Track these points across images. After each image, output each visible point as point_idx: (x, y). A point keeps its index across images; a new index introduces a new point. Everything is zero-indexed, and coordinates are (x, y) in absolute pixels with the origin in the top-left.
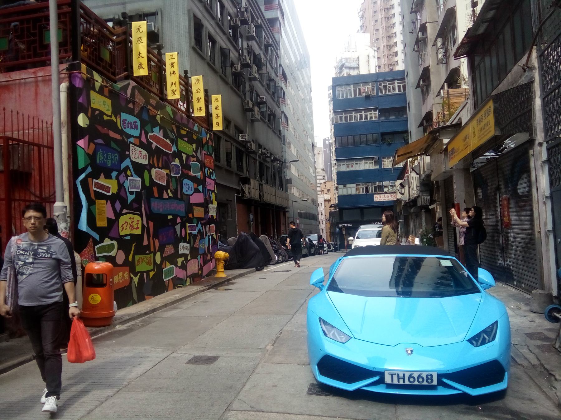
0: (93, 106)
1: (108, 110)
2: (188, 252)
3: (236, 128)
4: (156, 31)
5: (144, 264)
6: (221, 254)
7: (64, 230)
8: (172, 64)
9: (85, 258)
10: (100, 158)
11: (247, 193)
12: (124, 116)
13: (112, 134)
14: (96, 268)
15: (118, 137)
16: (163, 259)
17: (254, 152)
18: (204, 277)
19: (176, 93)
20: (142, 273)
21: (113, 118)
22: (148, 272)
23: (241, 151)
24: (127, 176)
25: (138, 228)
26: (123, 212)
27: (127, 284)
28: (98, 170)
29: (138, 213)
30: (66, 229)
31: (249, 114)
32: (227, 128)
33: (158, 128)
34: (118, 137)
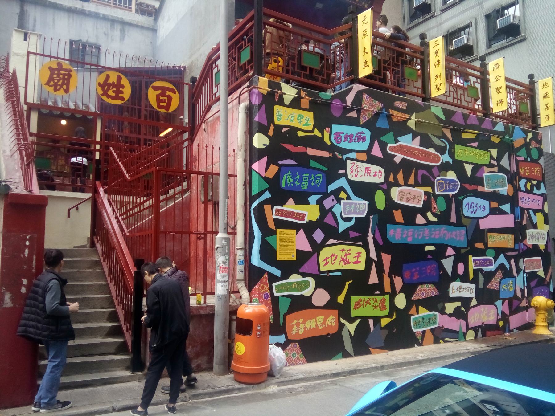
0: (277, 122)
1: (306, 124)
2: (473, 295)
4: (516, 22)
5: (367, 307)
6: (540, 300)
7: (222, 264)
8: (437, 53)
9: (255, 297)
10: (287, 180)
12: (336, 128)
13: (311, 152)
14: (247, 311)
15: (325, 154)
16: (410, 303)
18: (510, 331)
19: (441, 87)
20: (364, 320)
21: (317, 133)
22: (377, 320)
24: (339, 200)
25: (357, 262)
26: (328, 243)
27: (334, 331)
28: (279, 196)
29: (361, 243)
30: (224, 263)
33: (410, 135)
34: (325, 154)
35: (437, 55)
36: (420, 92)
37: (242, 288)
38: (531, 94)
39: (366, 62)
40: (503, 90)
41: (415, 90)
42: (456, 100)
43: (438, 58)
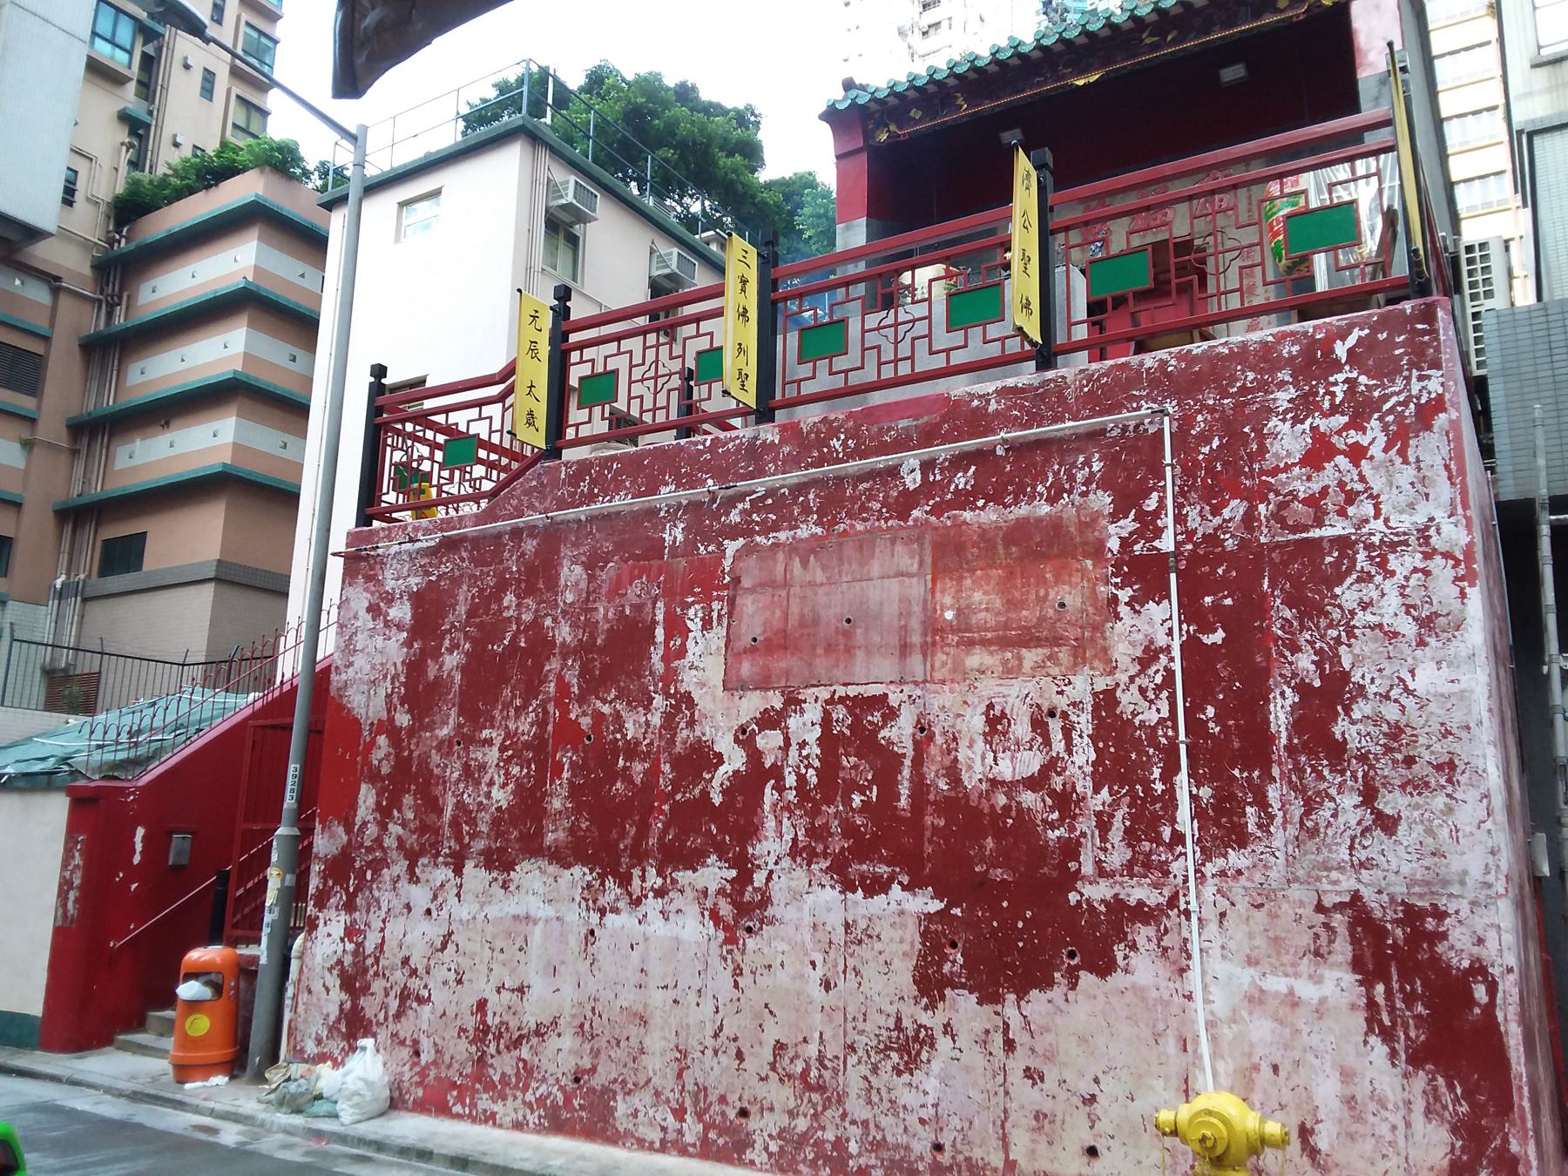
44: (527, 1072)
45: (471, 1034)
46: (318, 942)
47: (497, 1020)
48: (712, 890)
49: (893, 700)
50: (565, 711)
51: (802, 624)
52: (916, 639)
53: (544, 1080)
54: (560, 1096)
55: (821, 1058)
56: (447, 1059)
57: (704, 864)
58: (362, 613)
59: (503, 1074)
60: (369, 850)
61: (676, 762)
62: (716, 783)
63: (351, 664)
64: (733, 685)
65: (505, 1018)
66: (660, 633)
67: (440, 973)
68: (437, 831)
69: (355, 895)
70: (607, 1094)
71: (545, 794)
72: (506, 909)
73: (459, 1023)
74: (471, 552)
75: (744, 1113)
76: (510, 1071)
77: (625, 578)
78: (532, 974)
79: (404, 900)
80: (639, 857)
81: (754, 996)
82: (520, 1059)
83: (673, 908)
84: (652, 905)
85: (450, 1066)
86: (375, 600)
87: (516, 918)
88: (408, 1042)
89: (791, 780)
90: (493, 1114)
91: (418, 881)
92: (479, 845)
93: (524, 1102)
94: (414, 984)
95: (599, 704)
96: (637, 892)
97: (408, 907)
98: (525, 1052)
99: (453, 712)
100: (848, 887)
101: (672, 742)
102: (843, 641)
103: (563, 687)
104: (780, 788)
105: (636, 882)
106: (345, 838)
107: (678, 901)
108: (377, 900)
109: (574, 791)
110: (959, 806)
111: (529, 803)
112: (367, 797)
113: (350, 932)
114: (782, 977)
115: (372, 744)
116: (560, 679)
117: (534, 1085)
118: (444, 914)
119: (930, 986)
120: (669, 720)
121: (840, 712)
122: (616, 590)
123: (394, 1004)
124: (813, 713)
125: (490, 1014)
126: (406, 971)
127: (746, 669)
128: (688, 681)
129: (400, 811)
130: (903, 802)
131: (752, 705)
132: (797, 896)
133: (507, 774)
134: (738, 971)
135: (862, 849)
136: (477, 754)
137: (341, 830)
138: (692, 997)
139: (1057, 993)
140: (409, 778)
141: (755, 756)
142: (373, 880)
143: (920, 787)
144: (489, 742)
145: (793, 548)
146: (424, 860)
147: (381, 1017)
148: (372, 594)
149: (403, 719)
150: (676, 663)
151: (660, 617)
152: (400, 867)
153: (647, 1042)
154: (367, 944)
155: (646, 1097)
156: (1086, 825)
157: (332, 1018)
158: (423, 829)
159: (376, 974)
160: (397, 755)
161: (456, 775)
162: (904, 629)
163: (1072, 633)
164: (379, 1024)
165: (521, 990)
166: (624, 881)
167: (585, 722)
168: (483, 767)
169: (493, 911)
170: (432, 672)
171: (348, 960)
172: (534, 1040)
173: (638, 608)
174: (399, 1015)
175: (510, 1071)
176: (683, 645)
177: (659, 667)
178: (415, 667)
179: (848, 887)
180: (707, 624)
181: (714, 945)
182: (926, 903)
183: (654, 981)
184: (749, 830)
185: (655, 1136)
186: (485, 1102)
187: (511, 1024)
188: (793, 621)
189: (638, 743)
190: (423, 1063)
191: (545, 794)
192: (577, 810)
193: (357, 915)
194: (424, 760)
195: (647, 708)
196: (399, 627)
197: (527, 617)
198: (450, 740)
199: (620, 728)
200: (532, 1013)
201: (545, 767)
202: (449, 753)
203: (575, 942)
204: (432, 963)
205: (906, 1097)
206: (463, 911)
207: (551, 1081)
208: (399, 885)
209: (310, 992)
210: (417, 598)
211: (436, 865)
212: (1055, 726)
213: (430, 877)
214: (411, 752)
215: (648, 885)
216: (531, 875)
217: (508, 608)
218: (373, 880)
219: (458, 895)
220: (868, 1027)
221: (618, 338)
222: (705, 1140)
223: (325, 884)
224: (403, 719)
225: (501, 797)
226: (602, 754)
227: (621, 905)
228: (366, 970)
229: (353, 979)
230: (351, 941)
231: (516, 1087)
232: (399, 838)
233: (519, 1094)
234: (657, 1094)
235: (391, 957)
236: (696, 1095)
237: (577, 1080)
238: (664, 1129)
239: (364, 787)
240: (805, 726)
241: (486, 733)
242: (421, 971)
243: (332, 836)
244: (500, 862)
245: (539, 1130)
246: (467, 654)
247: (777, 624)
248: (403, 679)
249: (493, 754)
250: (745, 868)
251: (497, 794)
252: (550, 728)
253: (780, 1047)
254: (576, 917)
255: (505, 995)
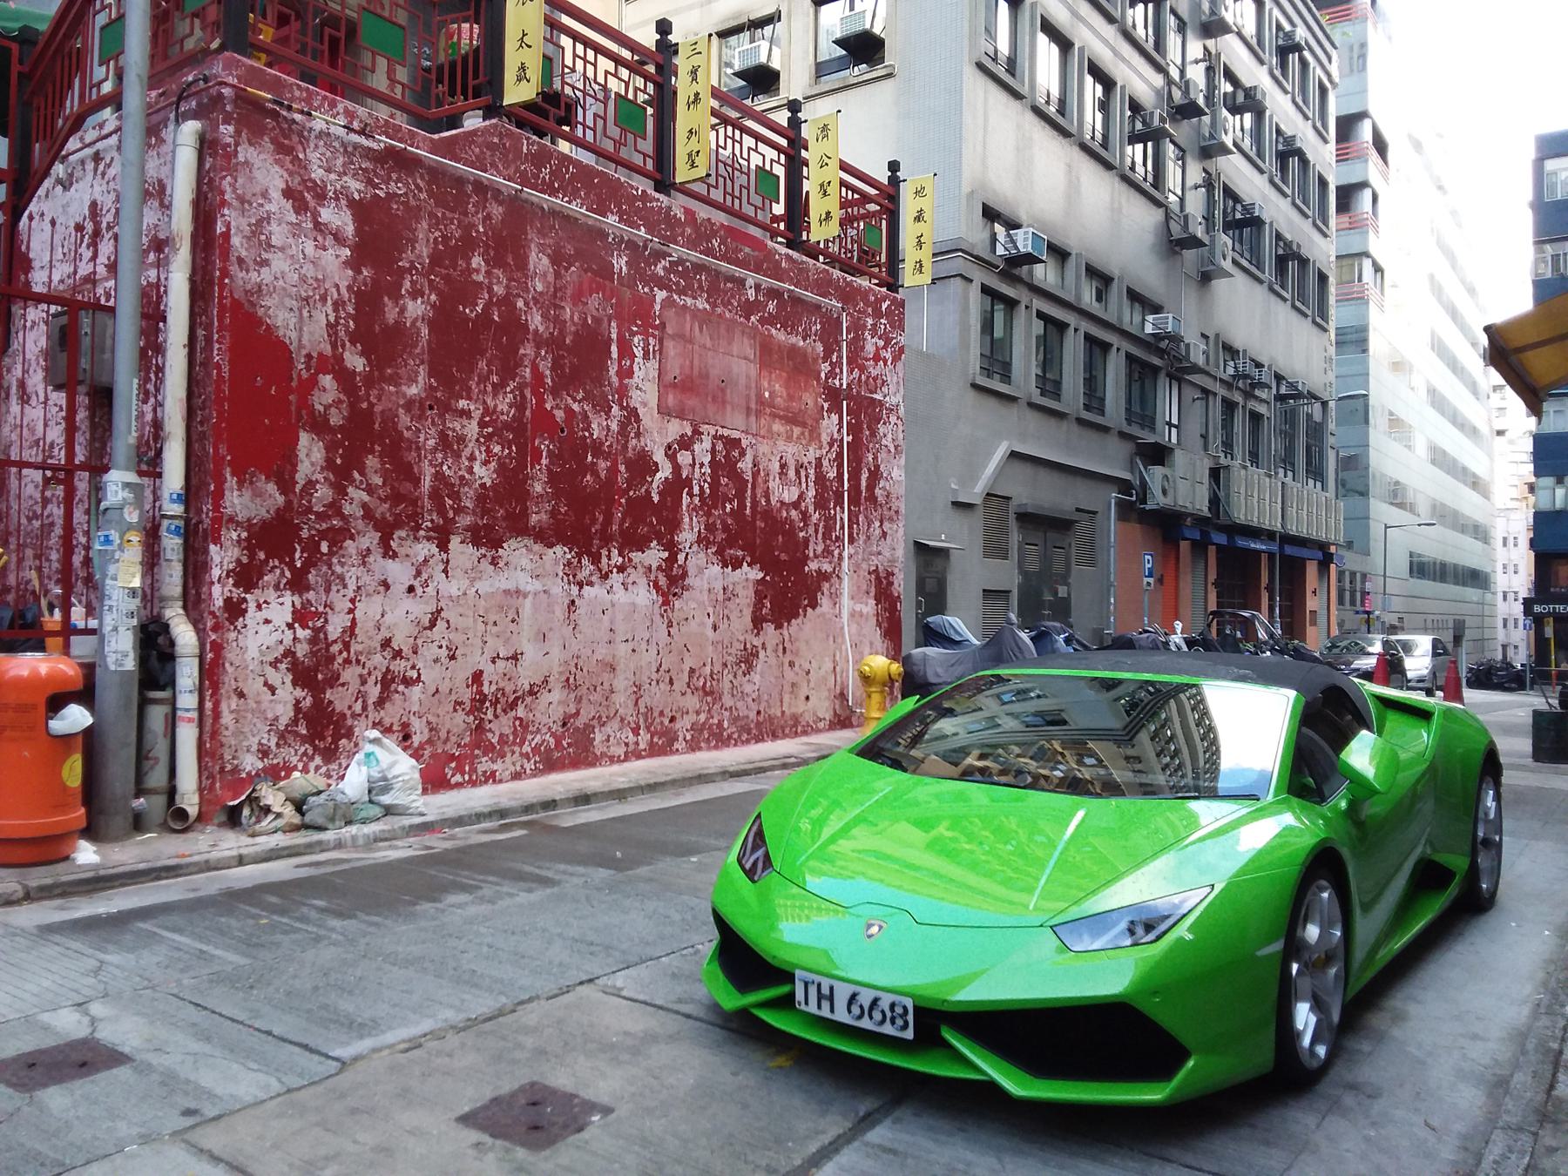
3: (1134, 296)
4: (877, 30)
11: (1158, 492)
17: (1196, 369)
23: (1145, 365)
31: (1189, 255)
32: (1099, 299)
35: (695, 79)
36: (650, 165)
37: (176, 620)
38: (890, 206)
39: (523, 68)
40: (834, 189)
41: (638, 160)
42: (729, 198)
43: (695, 88)
44: (524, 726)
45: (468, 706)
46: (250, 632)
47: (494, 688)
48: (654, 567)
49: (744, 443)
50: (541, 402)
51: (701, 376)
52: (753, 406)
53: (538, 730)
54: (552, 740)
55: (712, 673)
56: (443, 735)
57: (649, 548)
58: (276, 194)
59: (501, 735)
60: (321, 517)
61: (629, 464)
62: (655, 485)
63: (265, 263)
64: (664, 411)
65: (501, 685)
66: (614, 348)
67: (429, 652)
68: (414, 502)
69: (305, 569)
70: (588, 728)
71: (527, 477)
72: (497, 584)
73: (453, 697)
74: (429, 183)
75: (672, 719)
76: (507, 731)
77: (586, 286)
78: (525, 641)
79: (379, 577)
80: (606, 540)
81: (679, 640)
82: (516, 718)
83: (630, 580)
84: (616, 578)
85: (447, 739)
86: (295, 183)
87: (507, 592)
88: (395, 728)
89: (696, 490)
90: (493, 773)
91: (395, 556)
92: (465, 520)
93: (521, 754)
94: (399, 666)
95: (570, 401)
96: (605, 569)
97: (386, 585)
98: (521, 711)
99: (422, 371)
100: (725, 565)
101: (625, 447)
102: (719, 398)
103: (538, 376)
104: (691, 495)
105: (604, 560)
106: (281, 500)
107: (634, 575)
108: (342, 578)
109: (553, 479)
110: (768, 514)
111: (512, 483)
112: (310, 454)
113: (301, 616)
114: (693, 624)
115: (312, 383)
116: (535, 368)
117: (530, 737)
118: (430, 590)
119: (758, 622)
120: (623, 426)
121: (720, 447)
122: (578, 298)
123: (374, 692)
124: (707, 444)
125: (486, 684)
126: (388, 654)
127: (671, 400)
128: (636, 399)
129: (362, 474)
130: (748, 511)
131: (676, 428)
132: (701, 571)
133: (488, 451)
134: (670, 625)
135: (730, 542)
136: (455, 425)
137: (271, 488)
138: (644, 646)
139: (799, 620)
140: (359, 437)
141: (677, 468)
142: (331, 553)
143: (755, 503)
144: (466, 414)
145: (695, 313)
146: (403, 533)
147: (358, 708)
148: (291, 174)
149: (356, 361)
150: (626, 381)
151: (614, 336)
152: (370, 539)
153: (615, 683)
154: (330, 628)
155: (615, 724)
156: (811, 530)
157: (284, 721)
158: (396, 498)
159: (347, 661)
160: (352, 406)
161: (431, 442)
162: (748, 396)
163: (809, 422)
164: (355, 716)
165: (515, 658)
166: (596, 560)
167: (559, 415)
168: (461, 439)
169: (484, 586)
170: (391, 314)
171: (302, 650)
172: (529, 699)
173: (597, 320)
174: (380, 703)
175: (507, 731)
176: (631, 366)
177: (615, 379)
178: (367, 302)
179: (725, 565)
180: (646, 356)
181: (657, 606)
182: (755, 574)
183: (620, 637)
184: (675, 525)
185: (620, 751)
186: (484, 765)
187: (507, 690)
188: (696, 372)
189: (602, 444)
190: (416, 744)
191: (527, 477)
192: (556, 495)
193: (311, 595)
194: (390, 419)
195: (608, 417)
196: (338, 238)
197: (499, 290)
198: (421, 402)
199: (588, 428)
200: (526, 676)
201: (528, 454)
202: (421, 417)
203: (560, 612)
204: (419, 642)
205: (748, 688)
206: (452, 587)
207: (544, 730)
208: (371, 559)
209: (241, 695)
210: (360, 210)
211: (416, 539)
212: (803, 473)
213: (409, 551)
214: (372, 405)
215: (613, 562)
216: (517, 552)
217: (477, 271)
218: (331, 553)
219: (445, 571)
220: (733, 651)
221: (599, 50)
222: (651, 744)
223: (252, 556)
224: (356, 361)
225: (484, 474)
226: (574, 448)
227: (594, 579)
228: (332, 658)
229: (312, 670)
230: (304, 626)
231: (514, 743)
232: (364, 506)
233: (517, 749)
234: (622, 720)
235: (366, 639)
236: (646, 715)
237: (564, 725)
238: (627, 745)
239: (304, 438)
240: (702, 448)
241: (463, 404)
242: (406, 651)
243: (258, 494)
244: (487, 539)
245: (537, 773)
246: (433, 306)
247: (687, 371)
248: (350, 309)
249: (472, 429)
250: (672, 548)
251: (478, 469)
252: (528, 413)
253: (692, 671)
254: (558, 588)
255: (501, 664)
